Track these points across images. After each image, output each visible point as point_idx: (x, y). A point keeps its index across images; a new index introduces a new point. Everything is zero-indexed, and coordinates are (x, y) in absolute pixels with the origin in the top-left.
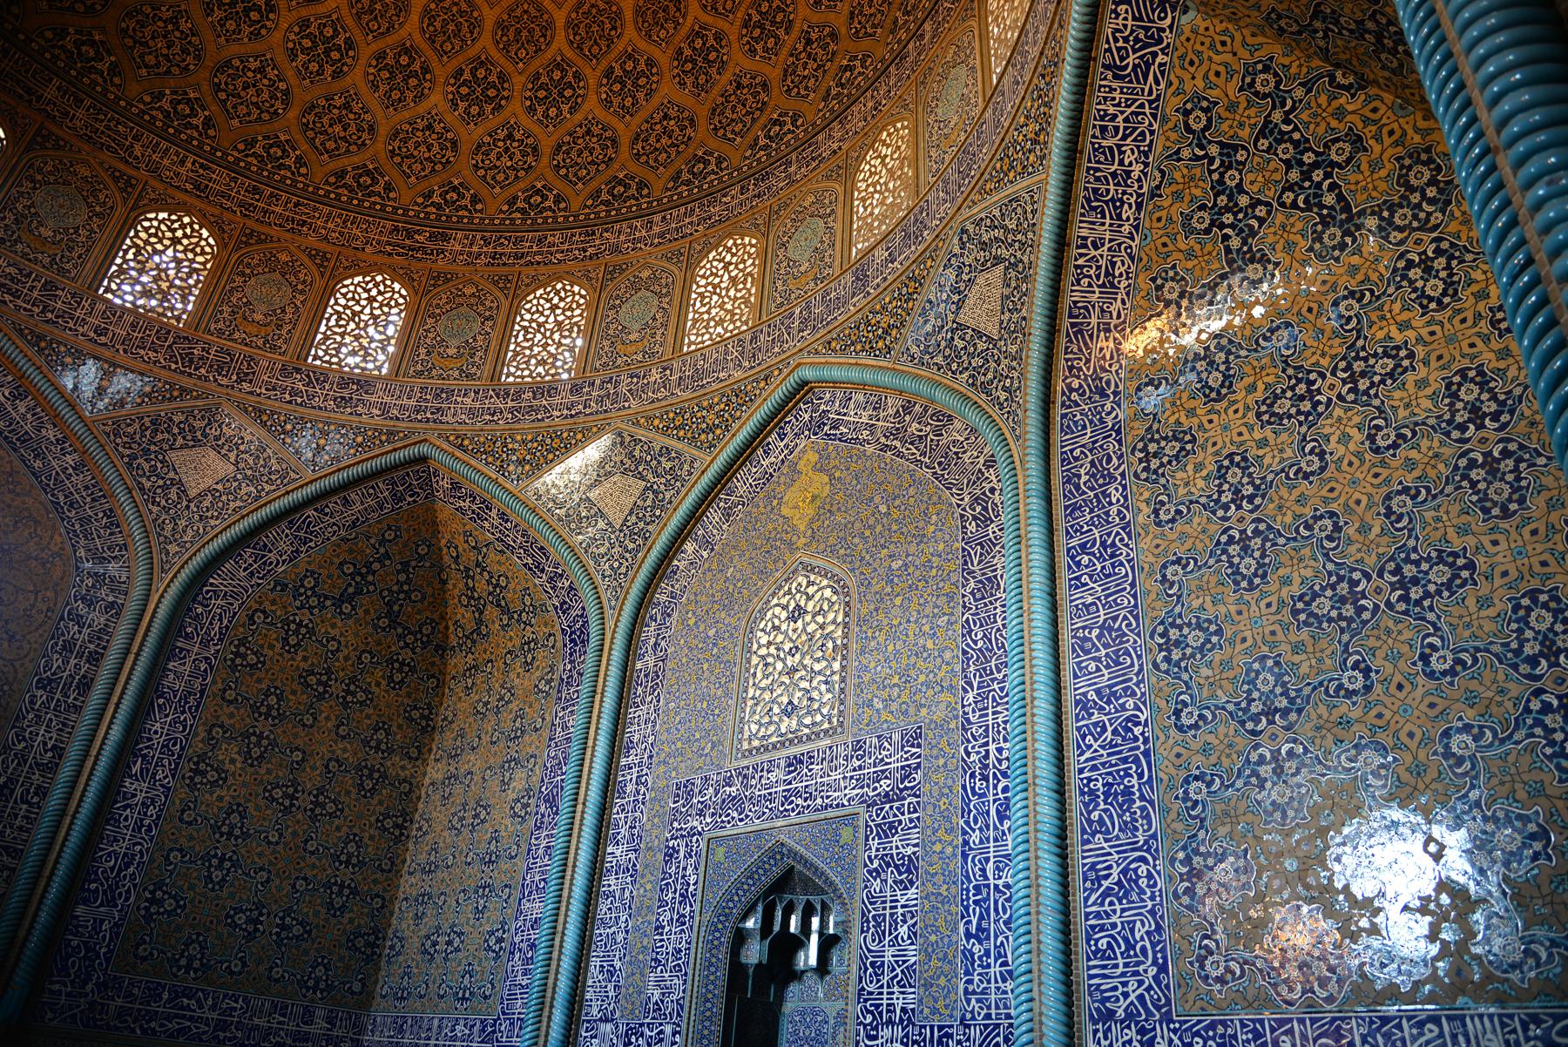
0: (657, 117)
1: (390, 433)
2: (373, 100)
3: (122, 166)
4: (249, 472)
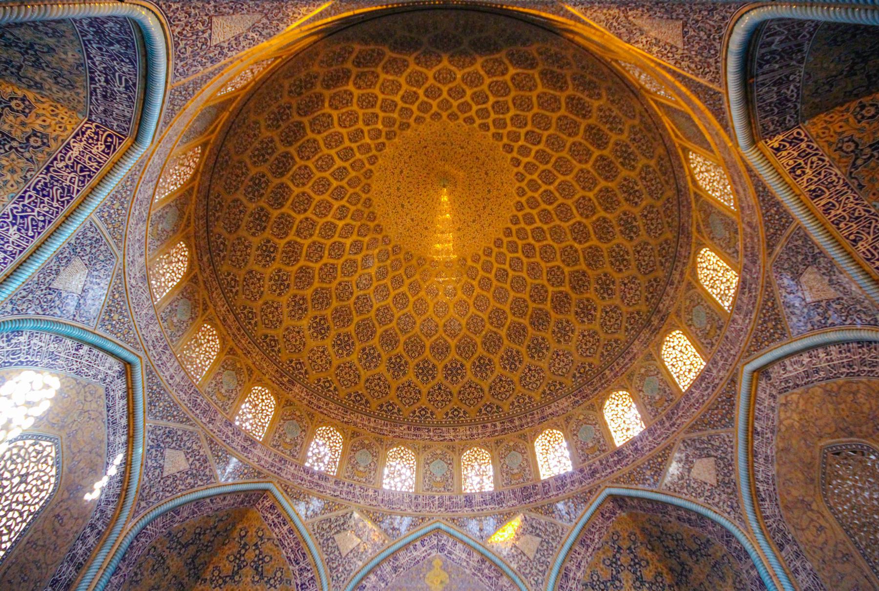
0: (377, 377)
1: (259, 473)
2: (286, 311)
3: (207, 299)
4: (195, 472)
